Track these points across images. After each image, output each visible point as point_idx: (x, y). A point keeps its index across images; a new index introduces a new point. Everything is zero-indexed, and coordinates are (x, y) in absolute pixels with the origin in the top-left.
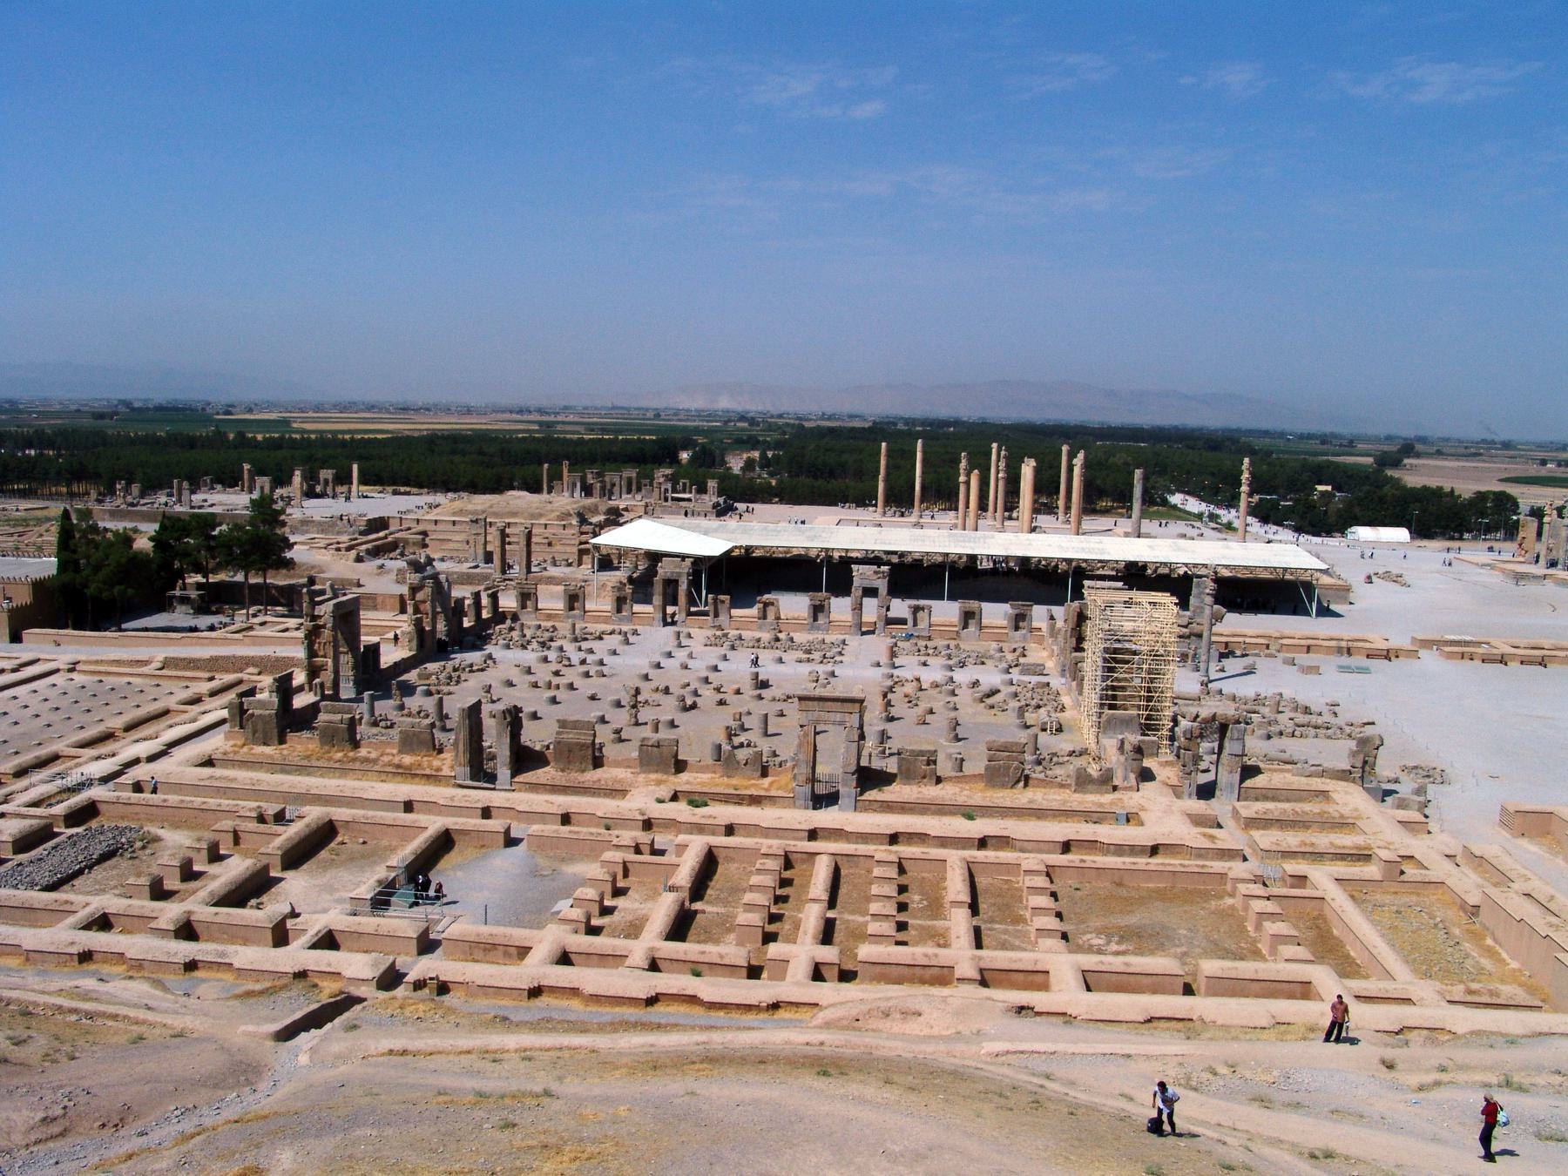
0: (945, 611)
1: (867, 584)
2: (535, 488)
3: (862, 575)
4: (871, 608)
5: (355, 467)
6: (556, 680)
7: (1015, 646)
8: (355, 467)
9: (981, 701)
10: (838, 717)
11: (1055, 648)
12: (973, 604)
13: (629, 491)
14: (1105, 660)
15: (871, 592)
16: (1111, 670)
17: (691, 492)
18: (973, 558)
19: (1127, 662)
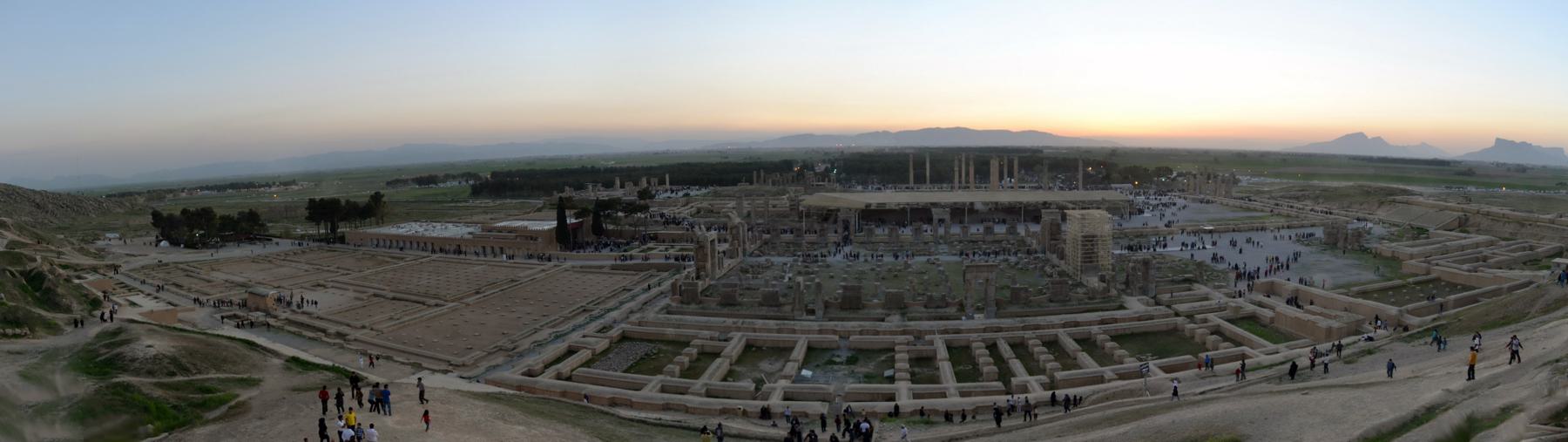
0: (976, 230)
1: (941, 217)
2: (751, 183)
3: (936, 213)
4: (941, 231)
5: (667, 177)
6: (810, 270)
7: (1012, 242)
8: (667, 177)
9: (1012, 267)
10: (986, 274)
11: (1034, 241)
12: (991, 223)
13: (793, 182)
14: (1082, 241)
15: (941, 221)
16: (1086, 245)
17: (823, 181)
18: (972, 204)
19: (1092, 241)
